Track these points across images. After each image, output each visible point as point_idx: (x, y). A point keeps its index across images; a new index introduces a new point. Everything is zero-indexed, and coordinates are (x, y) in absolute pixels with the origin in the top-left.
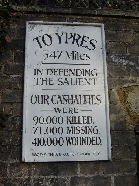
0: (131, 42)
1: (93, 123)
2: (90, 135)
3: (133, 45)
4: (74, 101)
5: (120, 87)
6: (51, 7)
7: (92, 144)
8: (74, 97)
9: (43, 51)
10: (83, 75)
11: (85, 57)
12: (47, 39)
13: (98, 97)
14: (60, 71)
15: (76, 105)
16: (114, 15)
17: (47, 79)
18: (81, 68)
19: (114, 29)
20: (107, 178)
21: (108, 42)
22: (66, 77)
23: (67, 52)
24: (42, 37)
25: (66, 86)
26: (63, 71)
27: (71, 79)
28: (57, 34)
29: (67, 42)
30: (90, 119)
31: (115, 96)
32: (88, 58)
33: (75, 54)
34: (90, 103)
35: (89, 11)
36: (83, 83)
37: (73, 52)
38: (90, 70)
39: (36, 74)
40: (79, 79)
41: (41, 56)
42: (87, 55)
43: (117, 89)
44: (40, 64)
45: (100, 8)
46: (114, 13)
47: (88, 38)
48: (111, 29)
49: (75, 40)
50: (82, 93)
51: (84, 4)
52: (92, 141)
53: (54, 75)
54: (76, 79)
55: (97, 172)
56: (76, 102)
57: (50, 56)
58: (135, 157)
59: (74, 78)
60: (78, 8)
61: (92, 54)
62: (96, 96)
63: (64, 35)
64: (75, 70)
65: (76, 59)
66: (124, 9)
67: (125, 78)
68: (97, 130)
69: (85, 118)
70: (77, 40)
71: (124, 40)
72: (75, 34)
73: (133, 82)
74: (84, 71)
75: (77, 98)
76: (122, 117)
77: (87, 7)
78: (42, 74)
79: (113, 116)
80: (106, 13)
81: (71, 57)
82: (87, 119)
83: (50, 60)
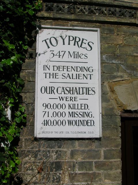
0: (122, 44)
1: (89, 109)
2: (86, 118)
3: (123, 47)
4: (74, 91)
5: (111, 81)
6: (57, 13)
7: (88, 126)
8: (74, 89)
9: (51, 51)
10: (82, 71)
11: (83, 57)
12: (54, 41)
13: (93, 89)
14: (63, 67)
15: (76, 95)
16: (109, 20)
17: (53, 74)
18: (81, 65)
19: (108, 33)
20: (98, 151)
21: (103, 44)
22: (68, 72)
23: (69, 52)
24: (49, 39)
25: (68, 80)
26: (66, 67)
27: (72, 74)
28: (61, 37)
29: (69, 44)
30: (86, 106)
31: (106, 88)
32: (86, 58)
33: (76, 54)
34: (86, 94)
35: (88, 17)
36: (82, 77)
37: (74, 52)
38: (87, 67)
39: (45, 70)
40: (79, 74)
41: (49, 55)
42: (86, 55)
43: (109, 82)
44: (47, 61)
45: (97, 14)
46: (108, 19)
47: (87, 40)
48: (105, 33)
49: (76, 42)
50: (81, 86)
51: (84, 11)
52: (87, 123)
53: (59, 70)
54: (76, 74)
55: (91, 146)
56: (76, 93)
57: (56, 55)
58: (120, 136)
59: (75, 73)
60: (79, 14)
61: (89, 54)
62: (91, 88)
63: (68, 37)
64: (76, 67)
65: (76, 58)
66: (117, 15)
67: (115, 74)
68: (92, 115)
69: (82, 105)
70: (77, 42)
71: (115, 43)
72: (76, 37)
73: (121, 77)
74: (83, 68)
75: (76, 89)
76: (111, 105)
77: (86, 13)
78: (49, 70)
79: (104, 103)
80: (102, 19)
81: (73, 56)
82: (84, 106)
83: (56, 58)
